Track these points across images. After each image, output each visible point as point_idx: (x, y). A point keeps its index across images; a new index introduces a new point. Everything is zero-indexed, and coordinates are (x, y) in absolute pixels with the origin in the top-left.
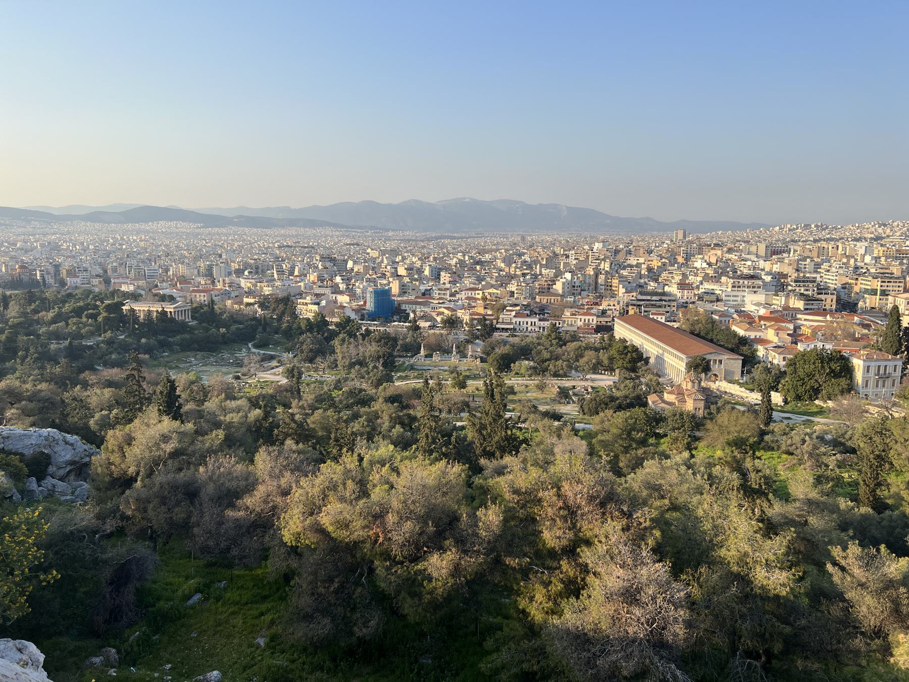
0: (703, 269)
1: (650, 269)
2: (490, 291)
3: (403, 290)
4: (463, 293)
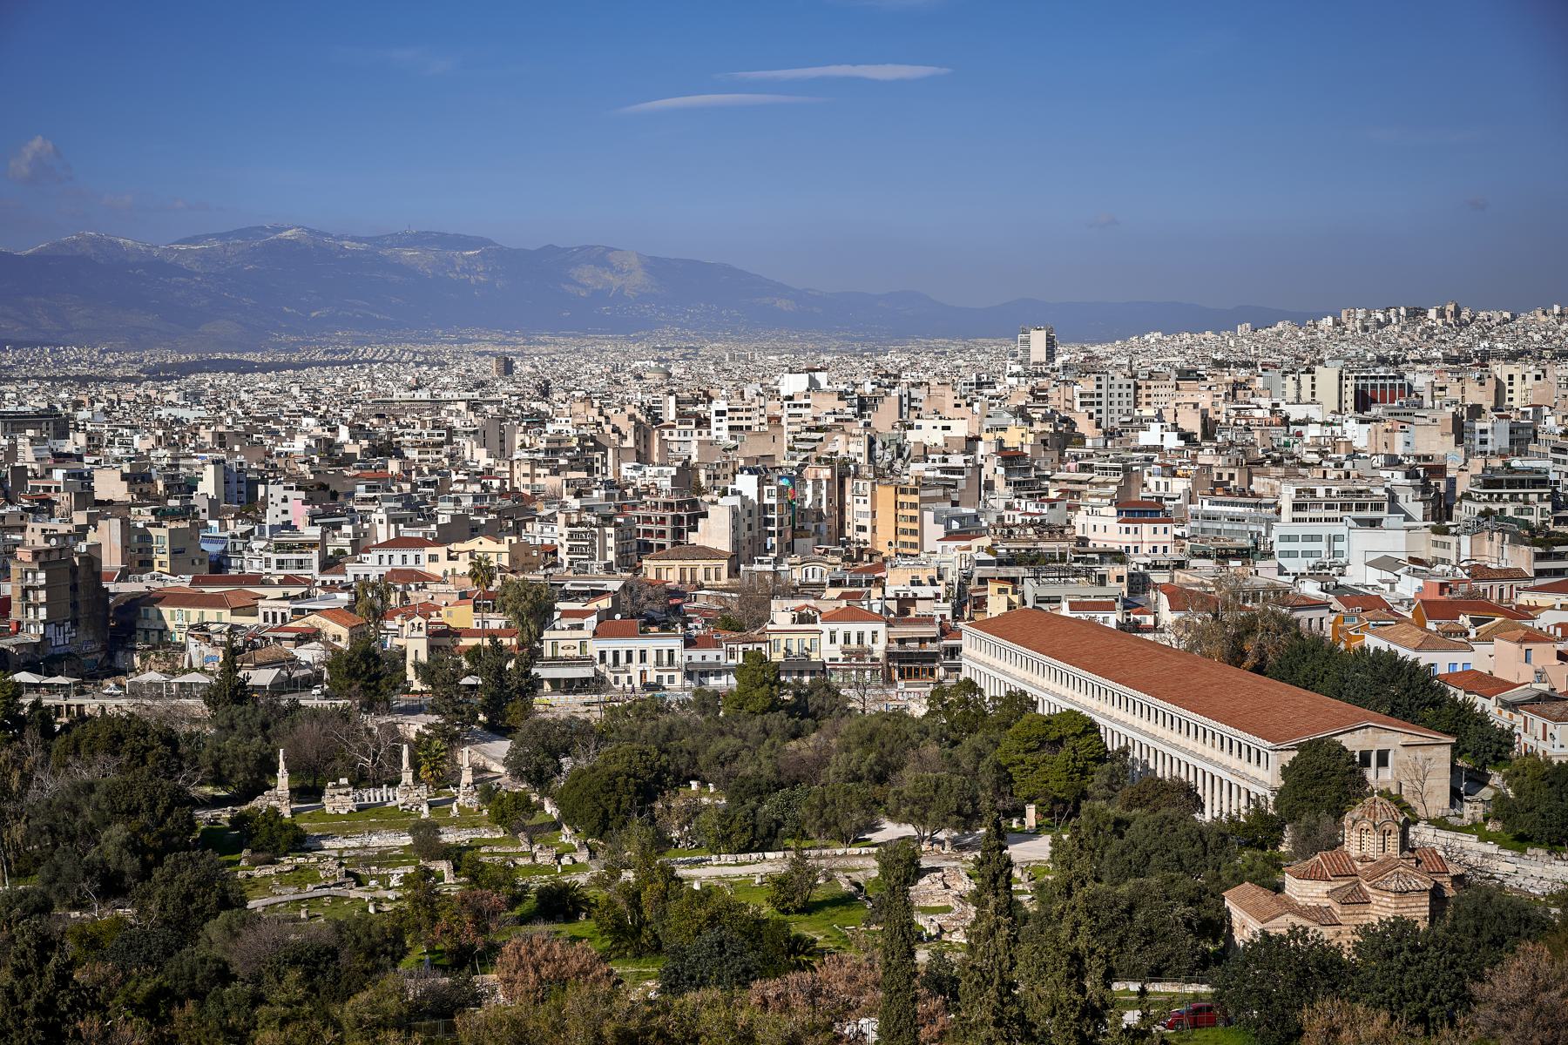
2: (472, 544)
4: (374, 555)
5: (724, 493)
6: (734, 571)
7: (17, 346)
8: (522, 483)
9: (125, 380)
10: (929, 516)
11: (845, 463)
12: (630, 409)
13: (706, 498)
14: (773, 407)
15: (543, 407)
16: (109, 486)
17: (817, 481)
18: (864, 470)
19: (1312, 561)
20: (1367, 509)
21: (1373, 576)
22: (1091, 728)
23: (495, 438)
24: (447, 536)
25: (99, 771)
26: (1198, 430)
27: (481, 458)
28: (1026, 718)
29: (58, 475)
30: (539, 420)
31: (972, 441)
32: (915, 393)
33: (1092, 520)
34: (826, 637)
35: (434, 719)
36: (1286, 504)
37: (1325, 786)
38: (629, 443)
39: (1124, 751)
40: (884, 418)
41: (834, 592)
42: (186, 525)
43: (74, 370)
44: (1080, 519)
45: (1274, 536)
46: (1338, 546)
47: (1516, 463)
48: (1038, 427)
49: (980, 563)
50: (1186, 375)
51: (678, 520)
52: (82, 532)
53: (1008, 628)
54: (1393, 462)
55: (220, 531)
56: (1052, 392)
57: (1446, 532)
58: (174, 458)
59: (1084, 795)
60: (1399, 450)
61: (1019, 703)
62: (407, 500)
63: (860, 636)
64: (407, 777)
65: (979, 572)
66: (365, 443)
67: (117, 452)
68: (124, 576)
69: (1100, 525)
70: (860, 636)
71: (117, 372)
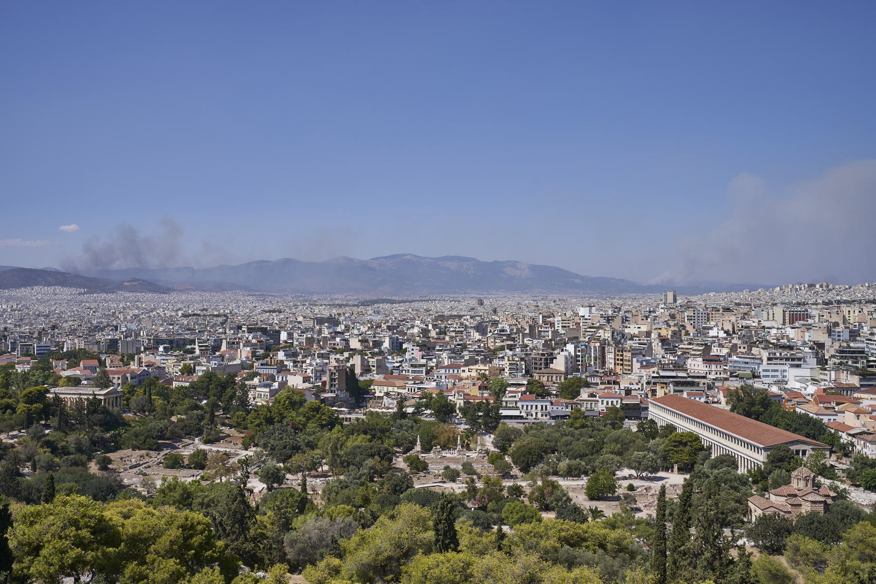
0: (726, 339)
1: (663, 341)
2: (476, 367)
3: (367, 370)
4: (443, 371)
5: (562, 350)
6: (565, 378)
7: (318, 294)
8: (491, 345)
9: (354, 306)
10: (635, 360)
11: (605, 340)
12: (527, 319)
13: (556, 352)
14: (577, 319)
15: (497, 318)
16: (355, 344)
17: (595, 347)
18: (612, 343)
19: (775, 379)
20: (797, 362)
21: (798, 385)
22: (697, 439)
23: (481, 329)
24: (467, 363)
25: (360, 440)
26: (731, 330)
27: (477, 336)
28: (673, 434)
29: (338, 339)
30: (495, 323)
31: (648, 334)
32: (627, 315)
33: (694, 362)
34: (600, 403)
35: (467, 427)
36: (765, 359)
37: (782, 461)
38: (527, 331)
39: (710, 448)
40: (617, 324)
41: (603, 387)
42: (380, 358)
43: (337, 302)
44: (689, 361)
45: (761, 370)
46: (785, 374)
47: (852, 345)
48: (672, 328)
49: (653, 377)
50: (727, 310)
51: (546, 359)
52: (348, 360)
53: (666, 401)
54: (804, 343)
55: (393, 361)
56: (677, 316)
57: (825, 370)
58: (374, 334)
59: (695, 463)
60: (807, 339)
61: (670, 428)
62: (452, 351)
63: (612, 402)
64: (459, 447)
65: (653, 381)
66: (437, 330)
67: (356, 332)
68: (362, 375)
69: (696, 365)
70: (612, 402)
71: (351, 303)
